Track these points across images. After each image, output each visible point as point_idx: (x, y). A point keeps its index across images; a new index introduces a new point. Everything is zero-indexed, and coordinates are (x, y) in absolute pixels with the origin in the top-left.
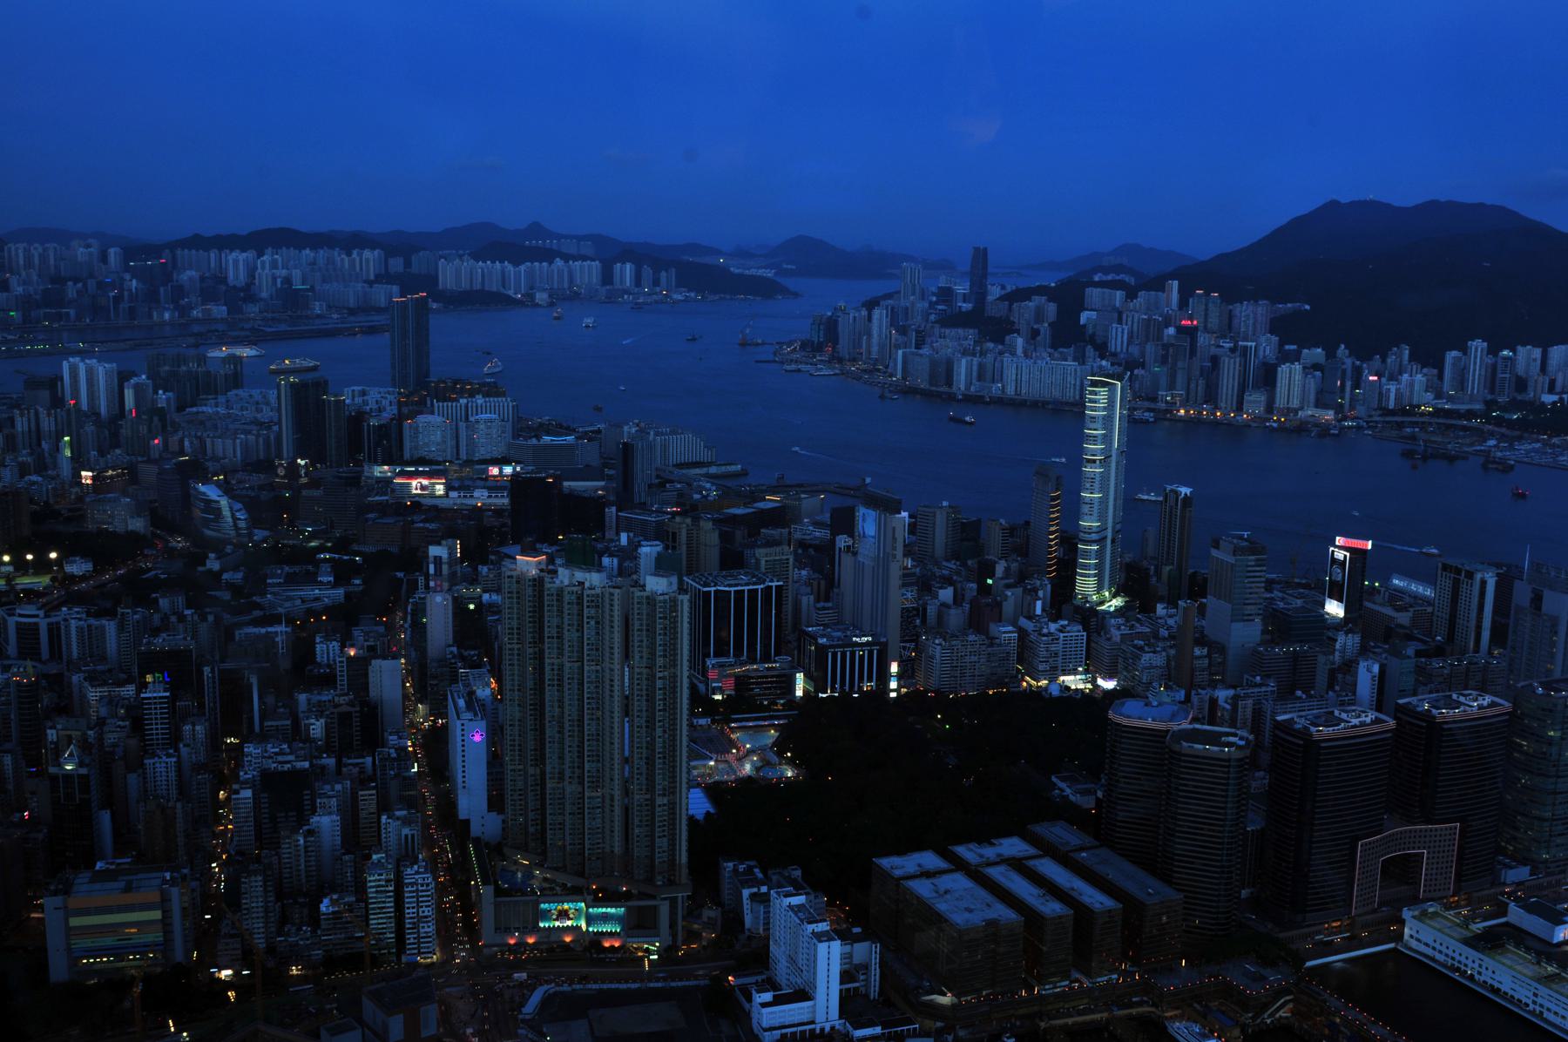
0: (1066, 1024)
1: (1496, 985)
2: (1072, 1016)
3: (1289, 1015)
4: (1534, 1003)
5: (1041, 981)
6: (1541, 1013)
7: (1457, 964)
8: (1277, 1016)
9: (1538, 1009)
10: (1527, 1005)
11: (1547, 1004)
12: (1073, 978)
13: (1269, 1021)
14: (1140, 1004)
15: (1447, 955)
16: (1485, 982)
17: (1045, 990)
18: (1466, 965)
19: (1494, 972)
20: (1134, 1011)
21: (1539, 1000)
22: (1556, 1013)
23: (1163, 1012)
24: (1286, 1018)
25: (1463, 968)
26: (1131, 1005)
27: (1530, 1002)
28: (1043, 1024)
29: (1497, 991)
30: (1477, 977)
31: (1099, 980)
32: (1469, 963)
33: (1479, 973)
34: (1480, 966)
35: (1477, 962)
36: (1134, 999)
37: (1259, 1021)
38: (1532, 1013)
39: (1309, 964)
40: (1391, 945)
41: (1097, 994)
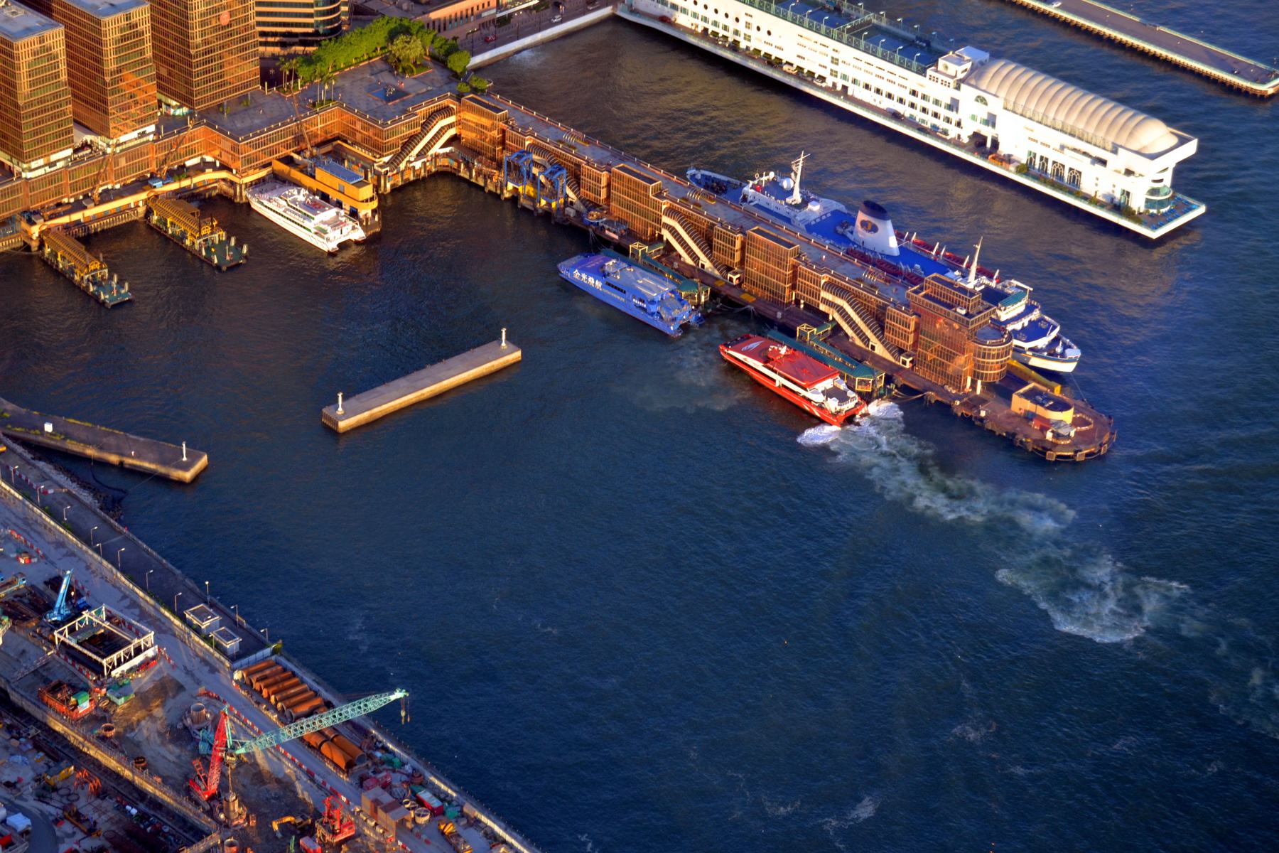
0: (77, 223)
1: (775, 54)
2: (85, 208)
3: (447, 150)
4: (834, 73)
5: (19, 155)
6: (845, 88)
7: (711, 28)
8: (432, 152)
9: (840, 83)
10: (822, 79)
11: (852, 74)
12: (78, 144)
13: (418, 165)
14: (201, 168)
15: (695, 15)
16: (757, 51)
17: (31, 170)
18: (725, 28)
19: (769, 33)
20: (185, 183)
21: (841, 69)
22: (867, 87)
23: (241, 173)
24: (447, 155)
25: (722, 32)
26: (182, 172)
27: (825, 73)
28: (35, 231)
29: (777, 64)
30: (743, 45)
31: (123, 139)
32: (732, 25)
33: (748, 38)
34: (748, 25)
35: (743, 19)
36: (188, 163)
37: (402, 166)
38: (832, 90)
39: (477, 60)
40: (606, 11)
41: (123, 162)
